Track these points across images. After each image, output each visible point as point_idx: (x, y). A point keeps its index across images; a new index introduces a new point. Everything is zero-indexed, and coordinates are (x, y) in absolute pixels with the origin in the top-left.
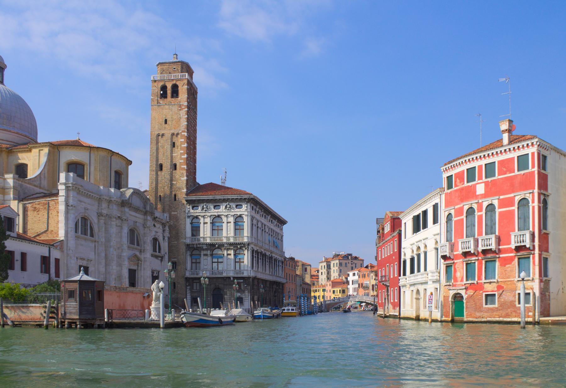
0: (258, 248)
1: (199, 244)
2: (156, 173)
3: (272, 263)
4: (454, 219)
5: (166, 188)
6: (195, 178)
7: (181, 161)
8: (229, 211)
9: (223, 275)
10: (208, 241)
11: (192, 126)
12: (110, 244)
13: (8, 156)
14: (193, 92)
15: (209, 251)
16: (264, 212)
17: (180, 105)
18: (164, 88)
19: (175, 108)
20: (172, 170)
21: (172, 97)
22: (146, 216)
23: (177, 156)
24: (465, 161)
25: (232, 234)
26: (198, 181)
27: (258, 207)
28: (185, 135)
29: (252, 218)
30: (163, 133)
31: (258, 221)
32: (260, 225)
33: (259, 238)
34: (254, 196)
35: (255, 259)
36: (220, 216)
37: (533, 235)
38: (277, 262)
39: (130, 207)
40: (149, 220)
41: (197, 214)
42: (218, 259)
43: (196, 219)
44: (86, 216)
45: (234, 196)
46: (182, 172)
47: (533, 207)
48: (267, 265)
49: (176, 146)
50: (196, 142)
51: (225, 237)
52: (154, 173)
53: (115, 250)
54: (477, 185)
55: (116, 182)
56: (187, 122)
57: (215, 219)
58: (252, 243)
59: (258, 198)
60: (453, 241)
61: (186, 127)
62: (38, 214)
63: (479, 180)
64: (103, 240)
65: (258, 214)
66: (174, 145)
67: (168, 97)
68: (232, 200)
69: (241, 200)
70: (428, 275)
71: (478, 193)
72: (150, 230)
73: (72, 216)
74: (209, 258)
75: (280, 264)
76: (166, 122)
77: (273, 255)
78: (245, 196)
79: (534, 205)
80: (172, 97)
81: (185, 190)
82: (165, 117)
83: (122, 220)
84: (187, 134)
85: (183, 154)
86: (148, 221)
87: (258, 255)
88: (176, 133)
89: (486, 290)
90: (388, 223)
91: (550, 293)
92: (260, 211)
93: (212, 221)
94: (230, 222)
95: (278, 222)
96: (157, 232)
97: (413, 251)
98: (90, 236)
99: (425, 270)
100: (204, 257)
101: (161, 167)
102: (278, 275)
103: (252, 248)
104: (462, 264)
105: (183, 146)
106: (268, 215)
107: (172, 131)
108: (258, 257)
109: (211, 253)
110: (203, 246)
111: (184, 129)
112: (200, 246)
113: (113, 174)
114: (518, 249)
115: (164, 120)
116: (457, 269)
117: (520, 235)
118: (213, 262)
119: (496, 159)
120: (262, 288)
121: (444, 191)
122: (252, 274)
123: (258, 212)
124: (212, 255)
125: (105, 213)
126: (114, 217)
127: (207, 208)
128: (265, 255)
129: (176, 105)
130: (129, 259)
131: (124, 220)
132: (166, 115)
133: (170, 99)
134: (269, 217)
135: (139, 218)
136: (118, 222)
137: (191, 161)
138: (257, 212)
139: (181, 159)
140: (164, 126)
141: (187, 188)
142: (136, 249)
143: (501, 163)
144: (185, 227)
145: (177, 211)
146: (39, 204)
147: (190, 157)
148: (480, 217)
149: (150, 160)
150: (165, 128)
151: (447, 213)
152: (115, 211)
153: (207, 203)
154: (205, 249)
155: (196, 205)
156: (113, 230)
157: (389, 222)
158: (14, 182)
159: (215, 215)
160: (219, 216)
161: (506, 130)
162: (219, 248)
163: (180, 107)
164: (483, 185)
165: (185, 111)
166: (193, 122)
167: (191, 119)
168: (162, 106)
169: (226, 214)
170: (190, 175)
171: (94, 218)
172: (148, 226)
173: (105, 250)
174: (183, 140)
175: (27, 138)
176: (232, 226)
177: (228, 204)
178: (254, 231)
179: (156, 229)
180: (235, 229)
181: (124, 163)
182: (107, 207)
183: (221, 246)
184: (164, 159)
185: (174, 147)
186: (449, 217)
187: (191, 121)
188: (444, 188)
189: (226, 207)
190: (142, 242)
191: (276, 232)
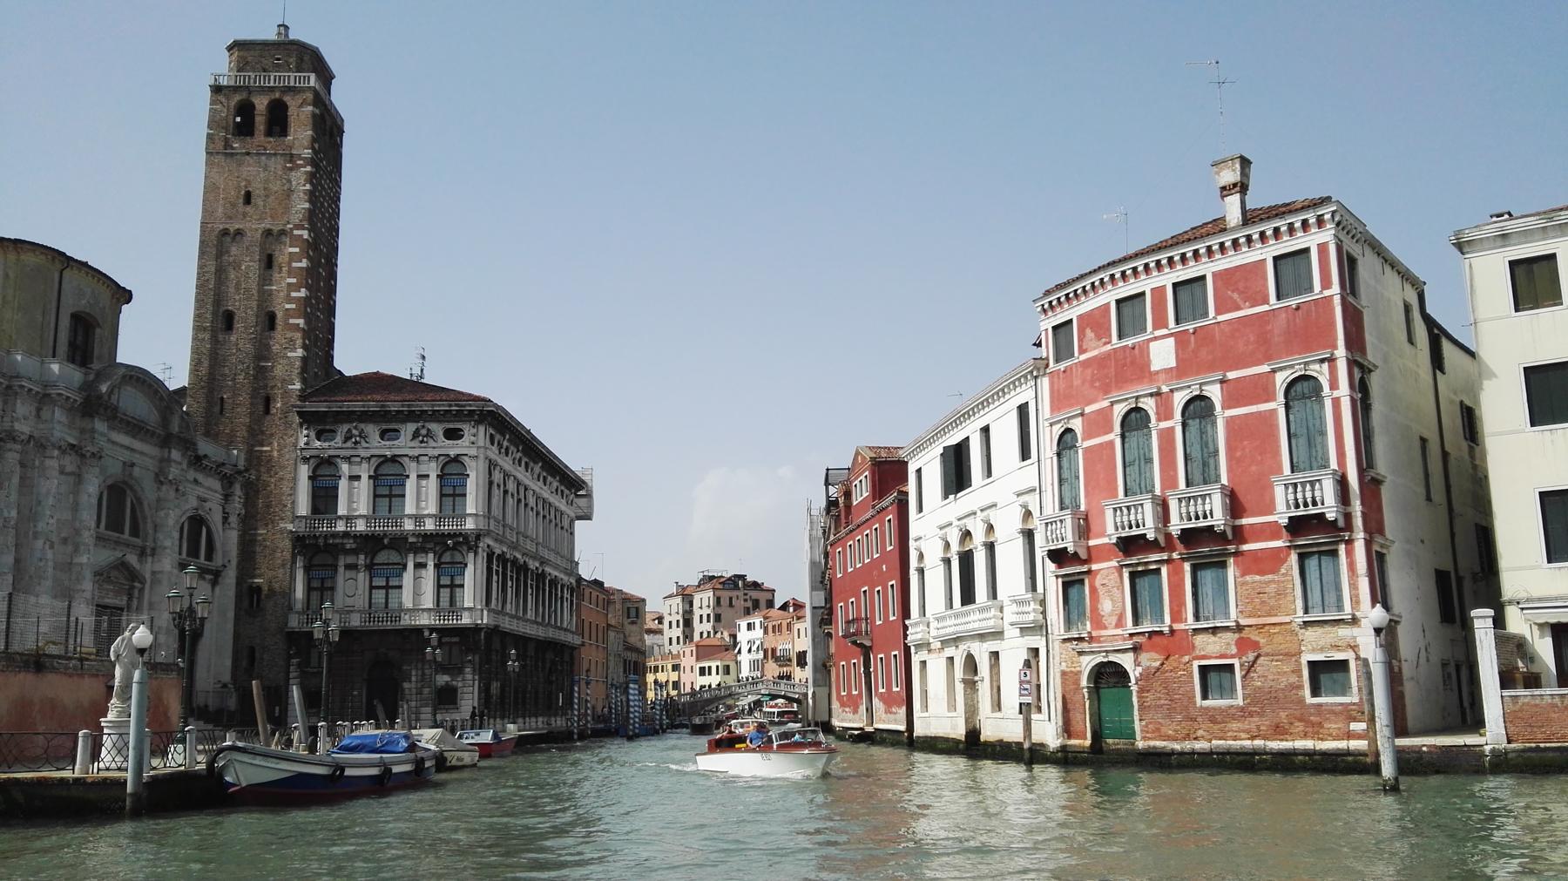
0: (505, 550)
1: (335, 535)
2: (212, 336)
3: (544, 590)
4: (1083, 444)
5: (242, 377)
6: (329, 358)
7: (288, 306)
8: (423, 445)
9: (402, 623)
10: (361, 526)
12: (35, 526)
14: (331, 129)
15: (362, 557)
16: (525, 453)
17: (292, 155)
18: (246, 109)
20: (263, 331)
21: (269, 133)
22: (167, 450)
23: (278, 291)
24: (1112, 276)
25: (431, 507)
26: (338, 364)
27: (507, 437)
28: (302, 235)
29: (492, 465)
30: (237, 227)
31: (506, 475)
32: (511, 486)
33: (509, 520)
34: (496, 405)
35: (495, 578)
36: (399, 459)
37: (1342, 483)
38: (556, 590)
39: (115, 417)
40: (175, 461)
41: (332, 452)
42: (387, 578)
43: (326, 465)
45: (439, 406)
46: (289, 335)
47: (1336, 403)
48: (529, 597)
49: (276, 268)
50: (336, 259)
51: (410, 517)
52: (207, 336)
53: (52, 547)
54: (1152, 345)
55: (72, 345)
56: (310, 201)
57: (383, 467)
58: (488, 533)
59: (507, 413)
60: (1083, 508)
61: (307, 215)
63: (1156, 327)
64: (14, 513)
65: (507, 455)
67: (257, 132)
68: (436, 416)
69: (461, 416)
70: (1001, 611)
71: (1155, 366)
72: (177, 490)
74: (362, 577)
75: (567, 595)
76: (248, 199)
77: (548, 569)
78: (470, 405)
79: (1336, 394)
80: (269, 133)
81: (298, 386)
82: (246, 187)
83: (83, 456)
84: (310, 235)
86: (173, 464)
87: (505, 568)
88: (276, 229)
89: (1203, 653)
90: (862, 477)
91: (1400, 661)
92: (512, 448)
93: (375, 471)
94: (428, 476)
95: (561, 482)
96: (203, 500)
97: (947, 546)
99: (993, 594)
100: (347, 572)
101: (228, 320)
102: (559, 624)
103: (488, 546)
104: (1116, 574)
105: (294, 265)
106: (536, 463)
107: (267, 224)
108: (504, 575)
109: (368, 561)
110: (345, 541)
112: (337, 541)
113: (65, 322)
114: (1297, 526)
115: (243, 192)
116: (1101, 591)
117: (1303, 484)
118: (372, 588)
119: (1207, 268)
120: (513, 657)
121: (1047, 365)
122: (486, 620)
123: (507, 449)
124: (370, 567)
125: (22, 433)
126: (53, 445)
127: (360, 436)
128: (522, 569)
130: (97, 574)
131: (88, 454)
132: (249, 182)
133: (262, 138)
134: (537, 469)
135: (145, 452)
136: (70, 463)
137: (319, 310)
138: (503, 450)
139: (289, 300)
140: (240, 210)
141: (304, 381)
142: (128, 545)
143: (1222, 277)
144: (294, 488)
147: (317, 298)
148: (1167, 435)
149: (197, 301)
150: (245, 215)
151: (1058, 430)
152: (60, 426)
153: (363, 422)
154: (351, 549)
155: (328, 427)
156: (51, 485)
157: (867, 473)
159: (386, 456)
160: (394, 459)
161: (1235, 185)
162: (391, 546)
163: (290, 162)
164: (1172, 340)
165: (306, 172)
166: (330, 206)
167: (324, 197)
168: (238, 157)
169: (416, 452)
170: (316, 346)
172: (170, 478)
173: (16, 545)
174: (297, 250)
176: (432, 485)
177: (423, 427)
178: (495, 501)
179: (200, 491)
180: (442, 495)
181: (105, 295)
182: (34, 413)
183: (400, 543)
184: (237, 298)
186: (1066, 441)
187: (322, 204)
188: (1047, 359)
189: (416, 435)
190: (150, 526)
191: (556, 510)
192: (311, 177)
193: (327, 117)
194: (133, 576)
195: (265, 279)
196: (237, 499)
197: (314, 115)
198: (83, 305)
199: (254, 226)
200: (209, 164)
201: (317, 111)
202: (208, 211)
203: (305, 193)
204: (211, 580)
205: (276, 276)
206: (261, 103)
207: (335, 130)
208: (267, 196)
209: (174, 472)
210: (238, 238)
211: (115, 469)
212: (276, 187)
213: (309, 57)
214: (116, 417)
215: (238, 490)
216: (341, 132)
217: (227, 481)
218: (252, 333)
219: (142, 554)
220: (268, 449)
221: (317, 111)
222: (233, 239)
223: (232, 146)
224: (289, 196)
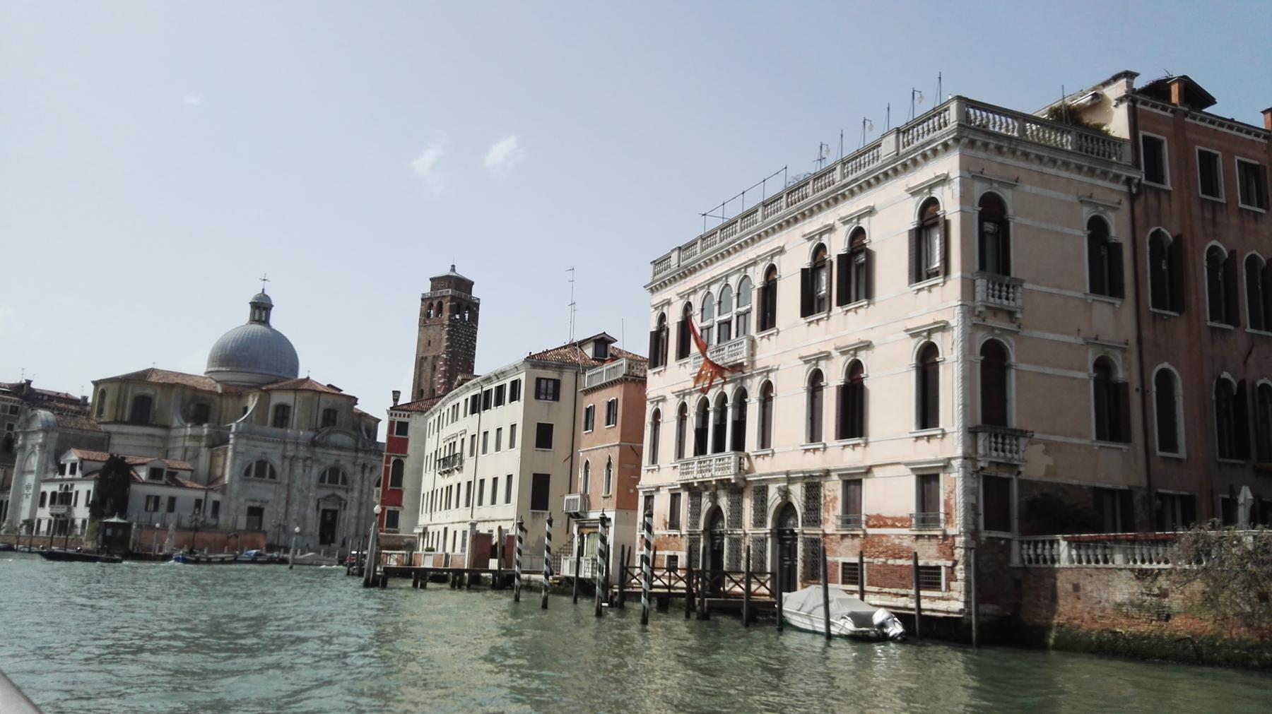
18: (431, 306)
64: (286, 481)
66: (434, 368)
73: (238, 462)
85: (440, 378)
107: (433, 354)
136: (309, 462)
152: (303, 452)
158: (209, 431)
171: (277, 461)
192: (448, 333)
194: (340, 499)
195: (433, 376)
197: (450, 305)
198: (329, 406)
199: (430, 355)
206: (435, 303)
209: (359, 461)
211: (330, 462)
212: (437, 338)
214: (325, 446)
216: (477, 305)
219: (347, 491)
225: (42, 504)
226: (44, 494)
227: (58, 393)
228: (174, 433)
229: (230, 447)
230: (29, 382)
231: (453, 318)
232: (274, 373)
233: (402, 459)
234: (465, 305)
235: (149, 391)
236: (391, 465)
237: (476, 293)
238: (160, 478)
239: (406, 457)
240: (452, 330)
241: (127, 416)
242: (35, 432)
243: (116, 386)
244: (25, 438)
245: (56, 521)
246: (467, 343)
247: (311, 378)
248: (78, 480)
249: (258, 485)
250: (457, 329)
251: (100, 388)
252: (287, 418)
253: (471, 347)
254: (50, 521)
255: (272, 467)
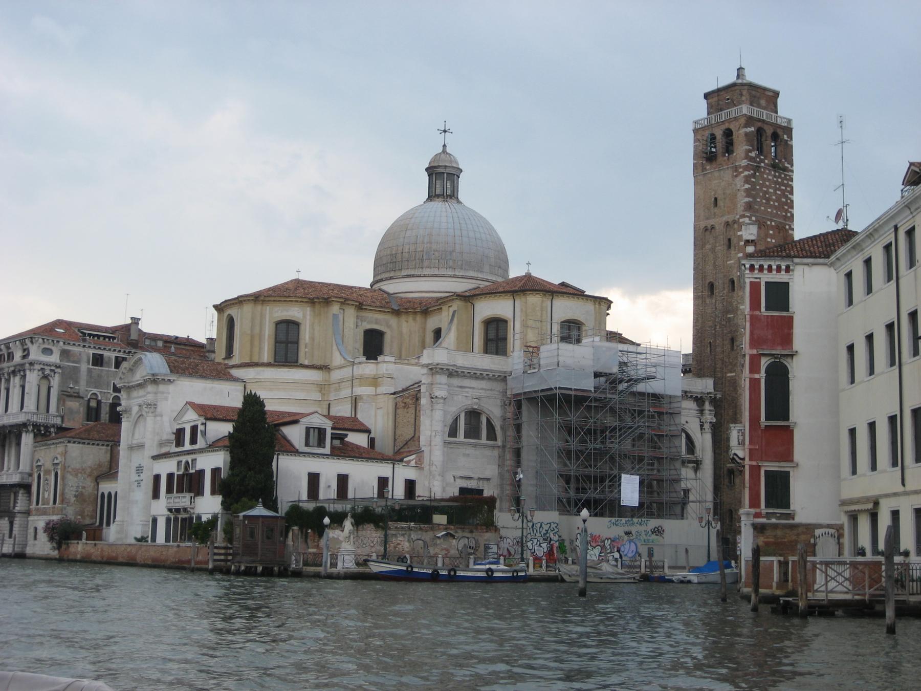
5: (718, 327)
11: (768, 200)
13: (426, 319)
19: (727, 175)
44: (476, 409)
49: (732, 248)
62: (408, 412)
73: (438, 414)
82: (714, 195)
88: (730, 220)
98: (488, 439)
107: (725, 219)
111: (743, 211)
115: (713, 199)
129: (729, 169)
145: (734, 371)
146: (408, 398)
150: (715, 213)
163: (736, 171)
166: (776, 190)
175: (474, 281)
185: (729, 246)
187: (767, 192)
193: (766, 127)
196: (707, 412)
199: (718, 222)
200: (696, 183)
201: (753, 129)
202: (697, 217)
203: (744, 191)
204: (694, 467)
205: (733, 252)
206: (719, 133)
207: (780, 132)
208: (725, 199)
210: (713, 231)
213: (746, 91)
215: (707, 406)
216: (788, 130)
217: (700, 400)
218: (722, 296)
220: (733, 374)
221: (753, 129)
222: (711, 232)
223: (706, 168)
224: (736, 195)
225: (156, 495)
226: (157, 478)
227: (177, 338)
228: (336, 375)
229: (423, 389)
230: (136, 321)
231: (753, 154)
232: (472, 274)
233: (787, 362)
234: (769, 131)
235: (294, 312)
236: (763, 374)
237: (785, 109)
238: (321, 443)
239: (792, 356)
240: (754, 176)
241: (266, 357)
242: (140, 386)
243: (247, 308)
244: (129, 398)
245: (176, 519)
246: (778, 200)
247: (535, 274)
248: (201, 451)
249: (470, 451)
250: (762, 174)
251: (226, 314)
252: (505, 339)
253: (786, 203)
254: (168, 520)
255: (488, 421)
